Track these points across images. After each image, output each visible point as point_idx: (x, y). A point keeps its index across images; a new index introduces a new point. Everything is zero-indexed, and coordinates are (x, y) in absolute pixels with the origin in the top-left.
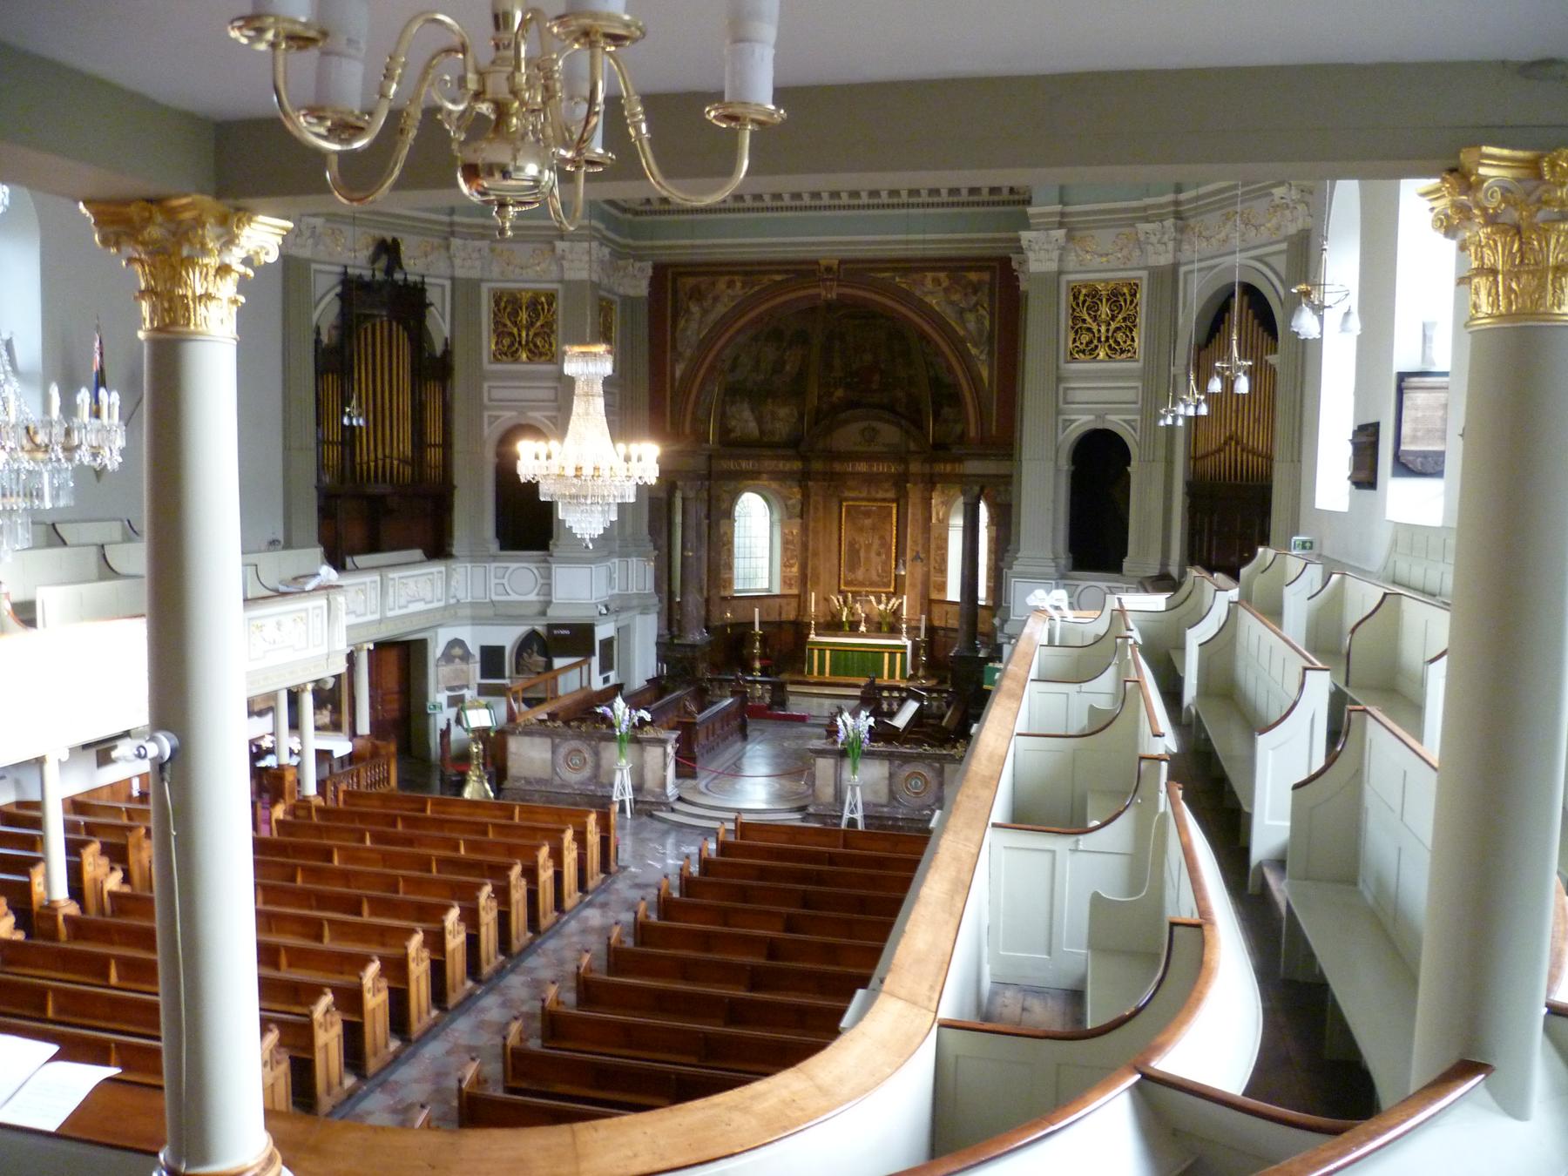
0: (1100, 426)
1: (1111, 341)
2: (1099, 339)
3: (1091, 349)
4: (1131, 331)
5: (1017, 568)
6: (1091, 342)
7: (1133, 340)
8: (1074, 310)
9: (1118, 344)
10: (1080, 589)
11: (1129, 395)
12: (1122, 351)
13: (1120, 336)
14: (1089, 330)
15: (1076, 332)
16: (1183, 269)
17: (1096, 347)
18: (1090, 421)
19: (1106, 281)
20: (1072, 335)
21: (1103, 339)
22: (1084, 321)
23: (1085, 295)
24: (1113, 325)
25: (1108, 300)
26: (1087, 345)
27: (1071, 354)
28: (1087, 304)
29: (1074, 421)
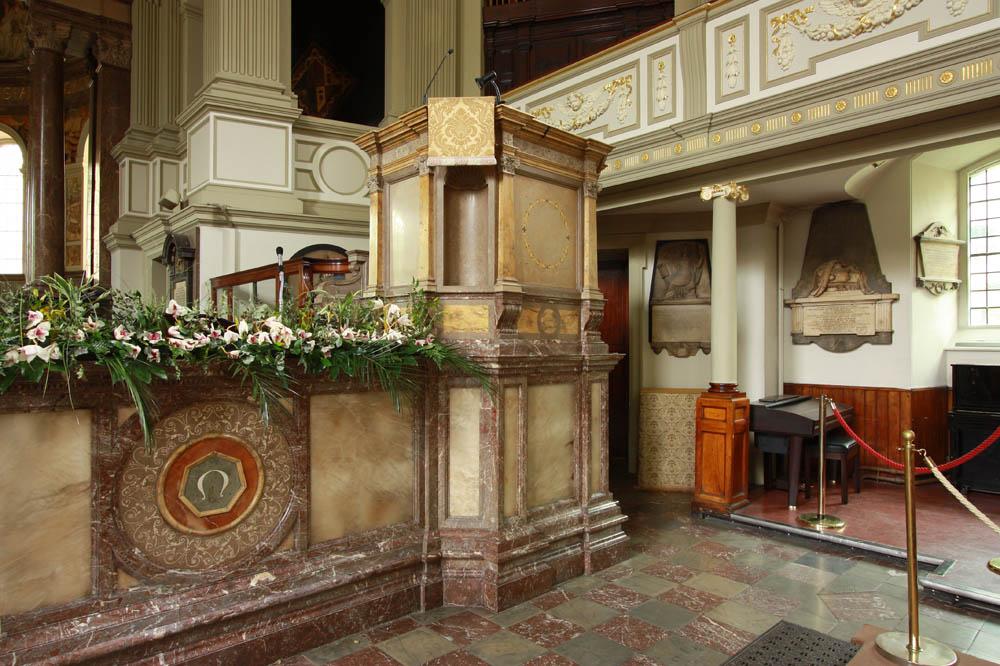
5: (217, 92)
10: (322, 151)
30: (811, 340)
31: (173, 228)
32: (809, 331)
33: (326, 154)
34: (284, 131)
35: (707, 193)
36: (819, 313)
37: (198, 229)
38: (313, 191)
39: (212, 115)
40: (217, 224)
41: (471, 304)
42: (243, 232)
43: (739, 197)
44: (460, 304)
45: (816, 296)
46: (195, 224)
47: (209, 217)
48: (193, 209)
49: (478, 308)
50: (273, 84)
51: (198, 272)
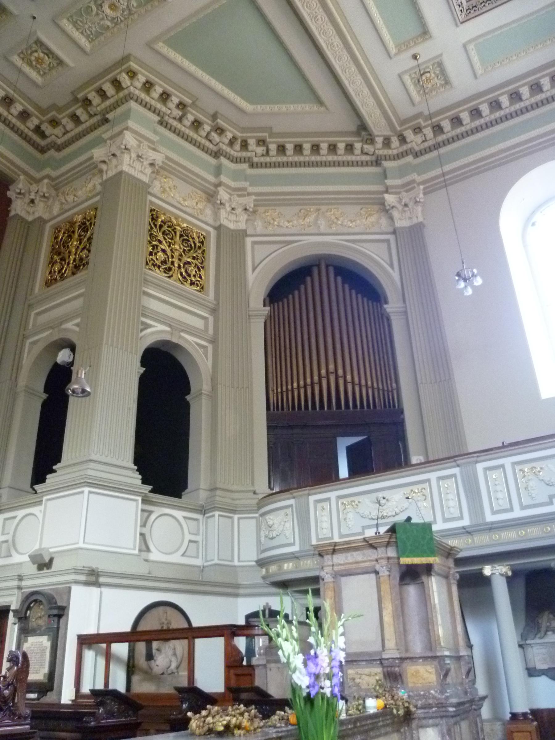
0: (175, 340)
1: (183, 270)
2: (173, 263)
3: (166, 269)
4: (199, 270)
6: (164, 262)
7: (200, 277)
8: (152, 228)
9: (189, 275)
10: (153, 517)
11: (199, 324)
12: (192, 284)
13: (192, 270)
14: (164, 251)
15: (154, 247)
16: (249, 241)
17: (170, 269)
18: (166, 332)
19: (185, 221)
20: (150, 249)
21: (176, 265)
22: (160, 242)
23: (162, 221)
24: (185, 259)
25: (181, 236)
26: (162, 262)
27: (147, 264)
28: (163, 229)
29: (150, 326)
30: (543, 673)
31: (24, 583)
32: (541, 666)
33: (157, 518)
34: (134, 503)
35: (487, 570)
36: (544, 651)
37: (70, 589)
38: (144, 551)
39: (86, 490)
40: (87, 584)
41: (423, 665)
42: (105, 590)
43: (507, 573)
44: (417, 665)
45: (541, 638)
46: (71, 582)
47: (83, 578)
48: (73, 571)
49: (429, 668)
50: (124, 464)
51: (66, 629)
